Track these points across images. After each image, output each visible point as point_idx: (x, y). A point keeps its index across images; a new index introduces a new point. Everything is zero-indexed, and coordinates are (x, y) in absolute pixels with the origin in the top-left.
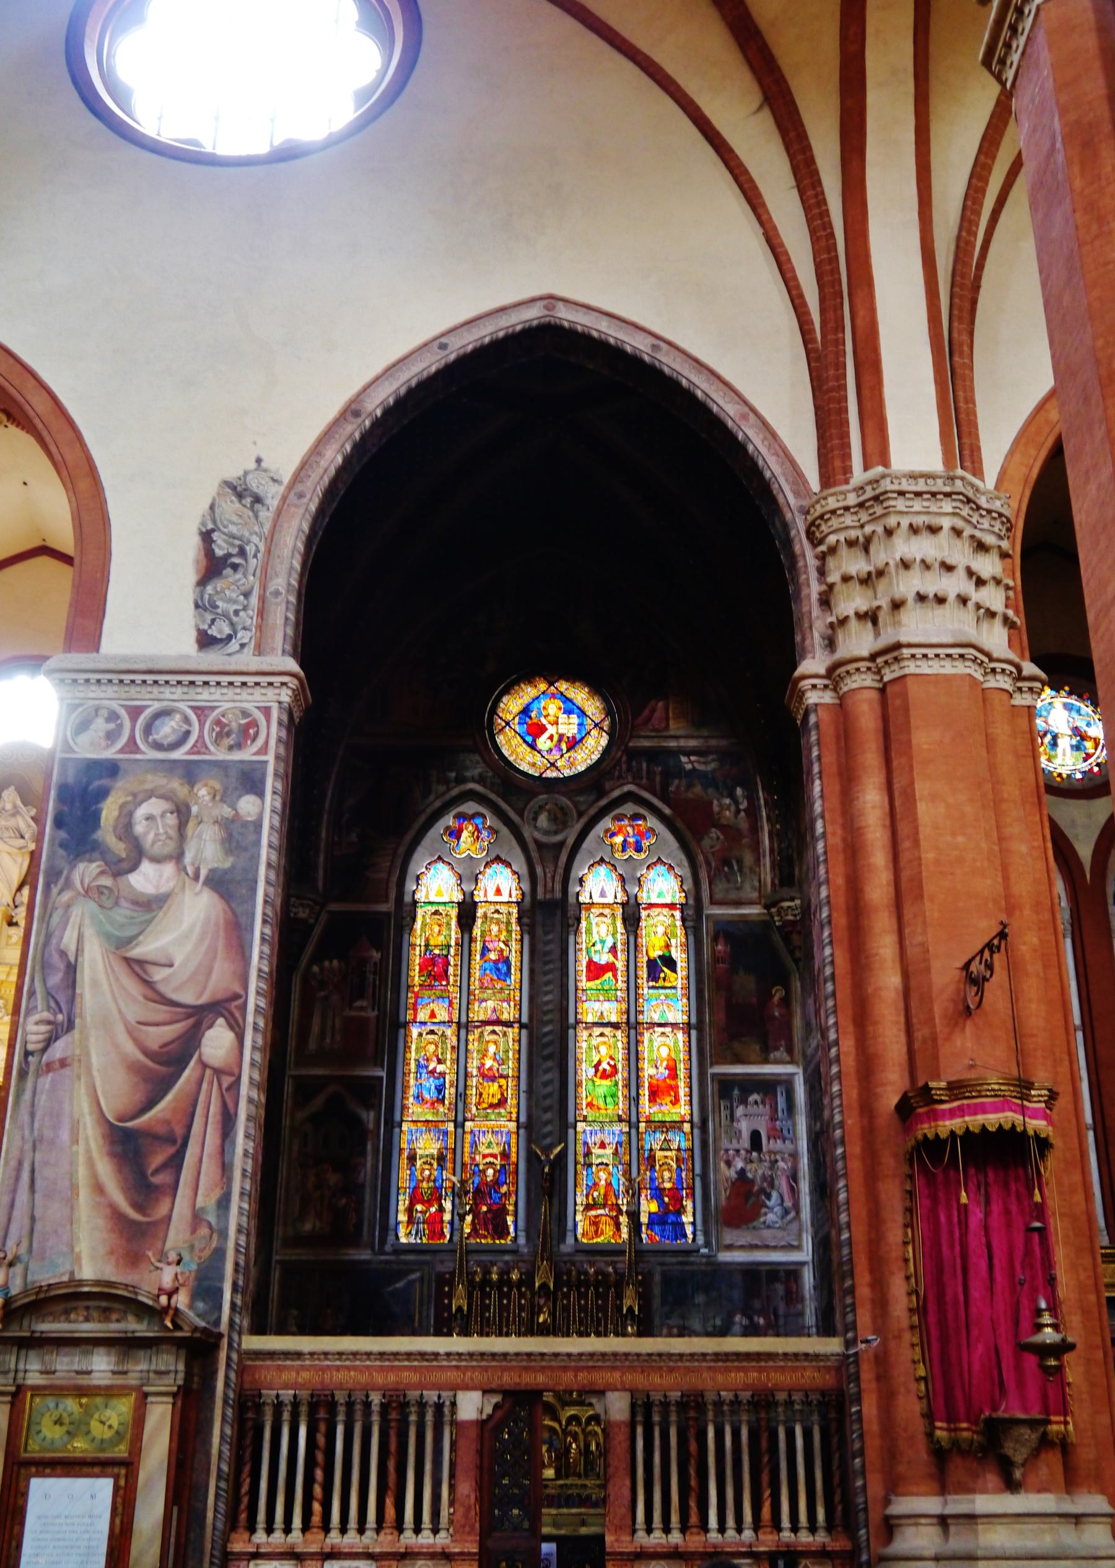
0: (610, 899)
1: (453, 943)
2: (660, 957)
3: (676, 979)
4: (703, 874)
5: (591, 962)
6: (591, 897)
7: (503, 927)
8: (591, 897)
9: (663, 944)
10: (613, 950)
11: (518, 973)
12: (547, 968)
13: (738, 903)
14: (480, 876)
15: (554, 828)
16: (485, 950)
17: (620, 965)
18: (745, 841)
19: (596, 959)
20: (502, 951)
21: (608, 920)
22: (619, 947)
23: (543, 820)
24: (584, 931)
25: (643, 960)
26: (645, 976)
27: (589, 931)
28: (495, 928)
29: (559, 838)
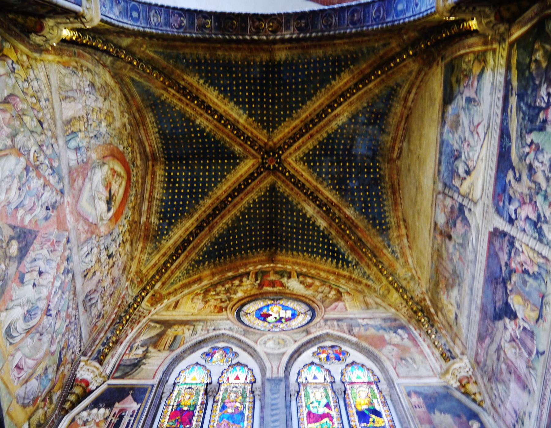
0: (322, 380)
1: (199, 403)
2: (366, 409)
3: (384, 422)
4: (388, 364)
5: (309, 413)
6: (306, 379)
7: (240, 395)
8: (306, 379)
9: (366, 401)
10: (327, 405)
11: (251, 421)
12: (274, 412)
13: (419, 377)
14: (225, 372)
15: (278, 347)
16: (224, 407)
17: (334, 413)
18: (412, 350)
19: (314, 411)
20: (237, 407)
21: (322, 390)
22: (332, 404)
23: (270, 344)
24: (303, 396)
25: (353, 412)
26: (357, 420)
27: (307, 396)
28: (233, 396)
29: (282, 351)
